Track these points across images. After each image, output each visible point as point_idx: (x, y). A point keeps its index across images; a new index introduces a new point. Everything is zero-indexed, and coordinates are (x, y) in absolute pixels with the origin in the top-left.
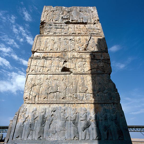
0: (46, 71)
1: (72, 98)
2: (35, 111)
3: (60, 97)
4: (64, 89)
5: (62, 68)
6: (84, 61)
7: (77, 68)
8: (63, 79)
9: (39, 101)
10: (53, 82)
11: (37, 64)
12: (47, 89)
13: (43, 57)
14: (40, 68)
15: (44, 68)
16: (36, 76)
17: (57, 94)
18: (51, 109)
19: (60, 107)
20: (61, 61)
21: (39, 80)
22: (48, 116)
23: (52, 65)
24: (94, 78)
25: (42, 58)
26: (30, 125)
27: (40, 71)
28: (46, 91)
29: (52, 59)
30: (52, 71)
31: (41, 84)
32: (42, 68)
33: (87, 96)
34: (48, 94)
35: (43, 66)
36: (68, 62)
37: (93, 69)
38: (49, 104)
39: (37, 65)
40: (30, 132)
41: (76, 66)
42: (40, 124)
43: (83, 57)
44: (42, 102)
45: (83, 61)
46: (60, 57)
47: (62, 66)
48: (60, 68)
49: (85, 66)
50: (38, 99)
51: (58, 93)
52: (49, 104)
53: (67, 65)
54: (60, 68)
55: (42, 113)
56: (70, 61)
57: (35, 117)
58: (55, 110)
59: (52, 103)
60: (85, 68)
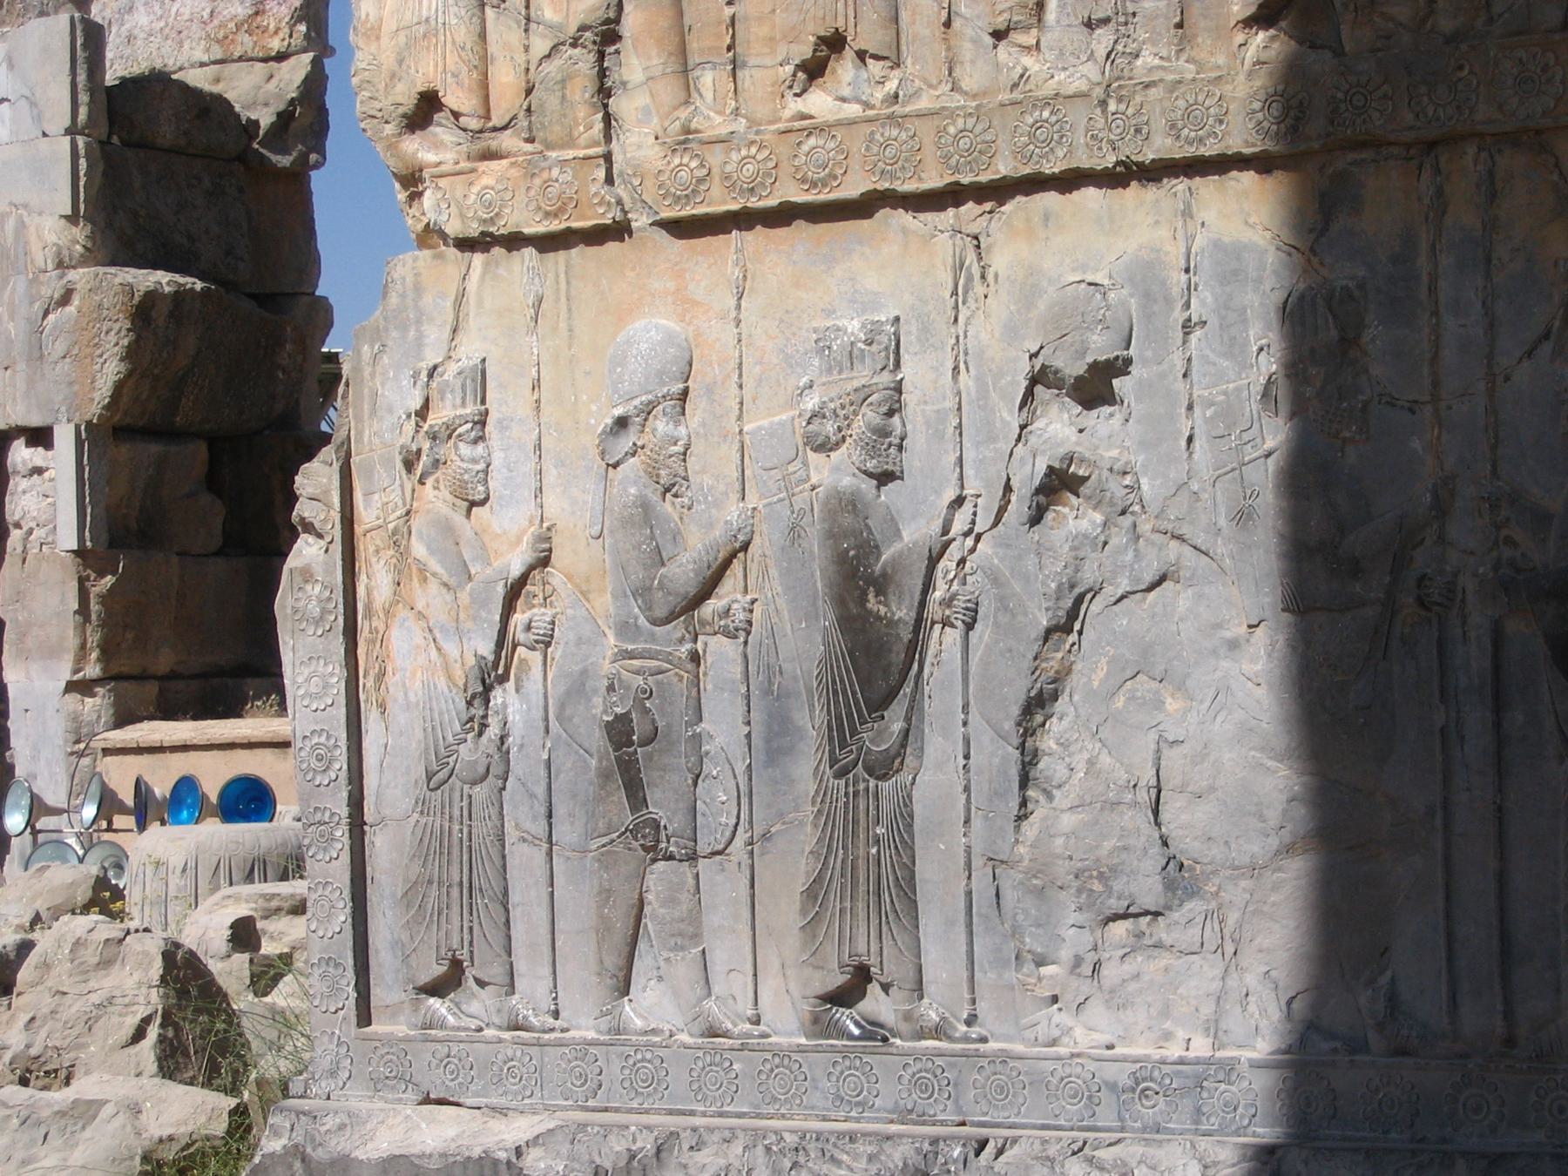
2: (661, 425)
9: (715, 157)
18: (1012, 332)
19: (1217, 245)
22: (959, 526)
26: (619, 732)
38: (950, 196)
40: (651, 880)
42: (810, 722)
44: (772, 176)
52: (950, 196)
55: (825, 447)
57: (683, 570)
58: (1101, 347)
59: (1004, 167)
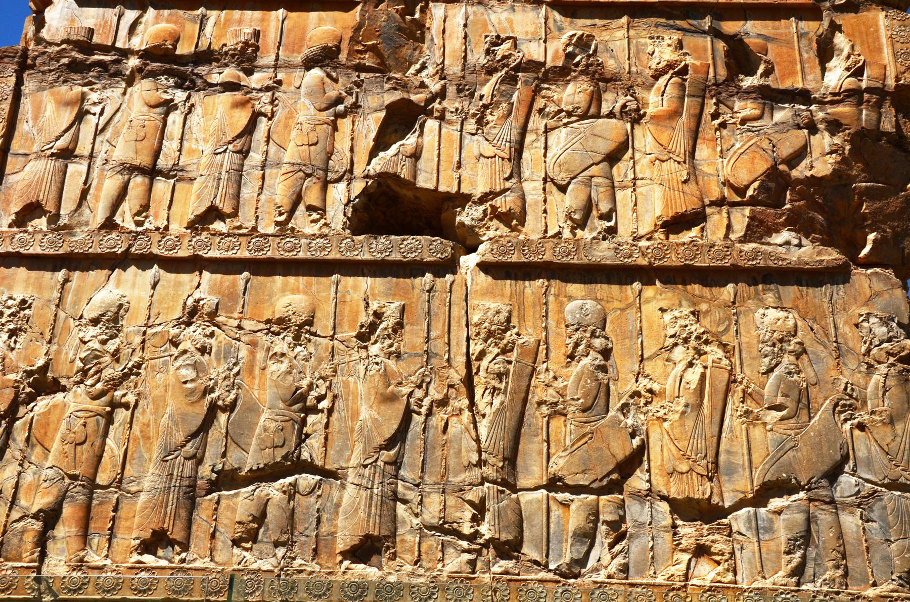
0: (177, 228)
1: (465, 544)
3: (324, 529)
4: (379, 441)
5: (358, 187)
6: (611, 115)
7: (532, 188)
8: (373, 327)
10: (252, 353)
11: (75, 140)
12: (180, 437)
13: (147, 55)
14: (110, 185)
15: (162, 187)
16: (67, 281)
17: (291, 498)
20: (350, 100)
21: (95, 322)
23: (256, 157)
24: (717, 314)
25: (133, 62)
27: (109, 225)
28: (169, 452)
29: (257, 80)
30: (246, 219)
31: (125, 376)
32: (138, 182)
33: (628, 526)
34: (193, 487)
35: (143, 160)
36: (432, 124)
37: (720, 203)
39: (84, 148)
41: (516, 172)
43: (611, 65)
45: (605, 109)
46: (343, 57)
47: (358, 171)
48: (338, 193)
49: (622, 170)
50: (75, 544)
51: (306, 480)
53: (416, 156)
54: (342, 186)
56: (451, 104)
60: (619, 195)
